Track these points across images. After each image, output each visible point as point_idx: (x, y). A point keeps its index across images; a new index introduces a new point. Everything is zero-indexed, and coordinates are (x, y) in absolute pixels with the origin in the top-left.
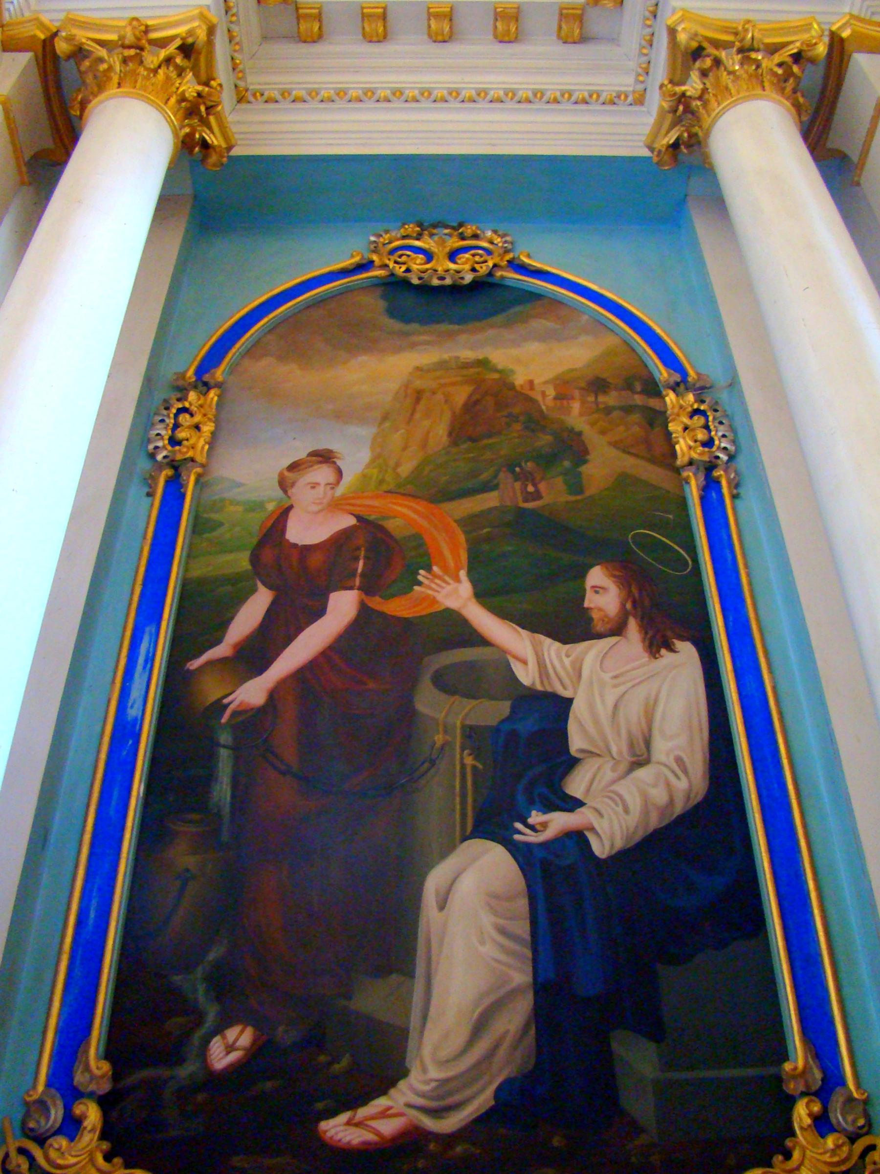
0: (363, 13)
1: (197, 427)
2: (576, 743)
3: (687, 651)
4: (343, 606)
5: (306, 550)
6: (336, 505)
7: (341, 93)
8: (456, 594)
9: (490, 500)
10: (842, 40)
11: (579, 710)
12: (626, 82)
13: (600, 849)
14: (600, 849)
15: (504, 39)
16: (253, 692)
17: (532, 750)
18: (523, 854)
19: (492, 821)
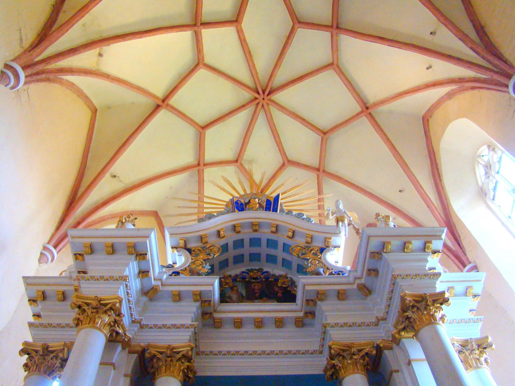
0: (235, 322)
7: (229, 352)
10: (380, 347)
12: (316, 347)
15: (278, 327)
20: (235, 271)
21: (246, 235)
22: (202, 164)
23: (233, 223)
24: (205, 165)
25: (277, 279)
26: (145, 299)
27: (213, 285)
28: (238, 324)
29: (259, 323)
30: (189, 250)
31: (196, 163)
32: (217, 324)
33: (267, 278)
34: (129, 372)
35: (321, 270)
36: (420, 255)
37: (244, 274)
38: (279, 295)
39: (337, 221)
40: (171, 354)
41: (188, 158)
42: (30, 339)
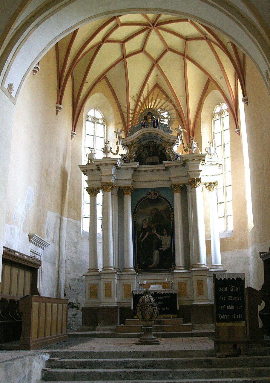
1: (135, 218)
2: (162, 243)
3: (170, 236)
4: (148, 233)
5: (145, 229)
6: (147, 224)
8: (155, 232)
9: (157, 224)
11: (163, 241)
13: (163, 250)
14: (163, 250)
16: (142, 241)
17: (160, 244)
18: (159, 251)
19: (157, 249)
20: (144, 143)
21: (147, 135)
22: (125, 57)
23: (142, 133)
24: (128, 56)
25: (159, 145)
26: (117, 170)
27: (137, 165)
28: (146, 171)
29: (152, 171)
30: (127, 146)
31: (122, 57)
32: (140, 171)
33: (155, 146)
34: (117, 194)
35: (171, 156)
36: (198, 162)
37: (147, 144)
38: (159, 154)
39: (178, 135)
40: (127, 188)
41: (117, 55)
42: (88, 187)
